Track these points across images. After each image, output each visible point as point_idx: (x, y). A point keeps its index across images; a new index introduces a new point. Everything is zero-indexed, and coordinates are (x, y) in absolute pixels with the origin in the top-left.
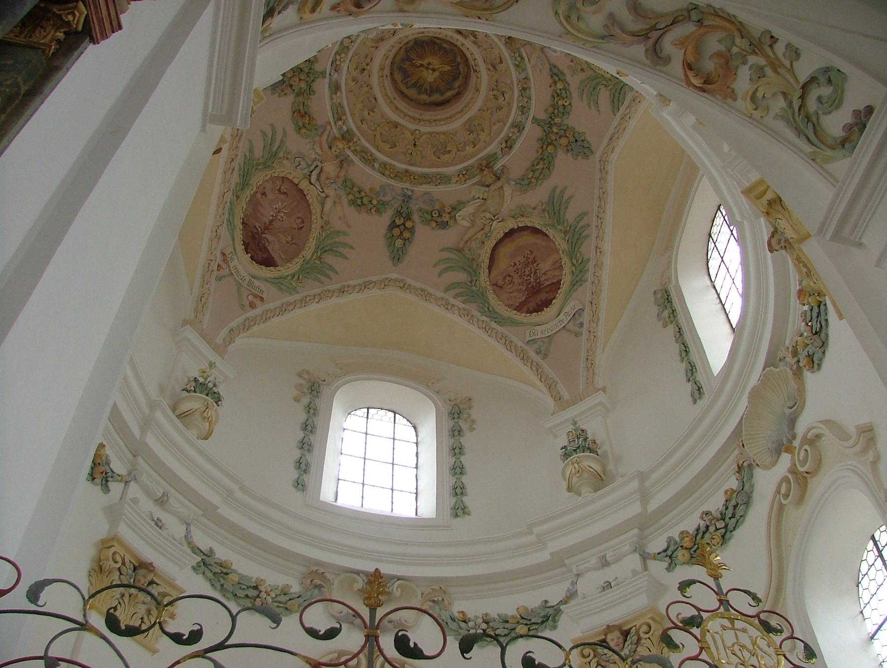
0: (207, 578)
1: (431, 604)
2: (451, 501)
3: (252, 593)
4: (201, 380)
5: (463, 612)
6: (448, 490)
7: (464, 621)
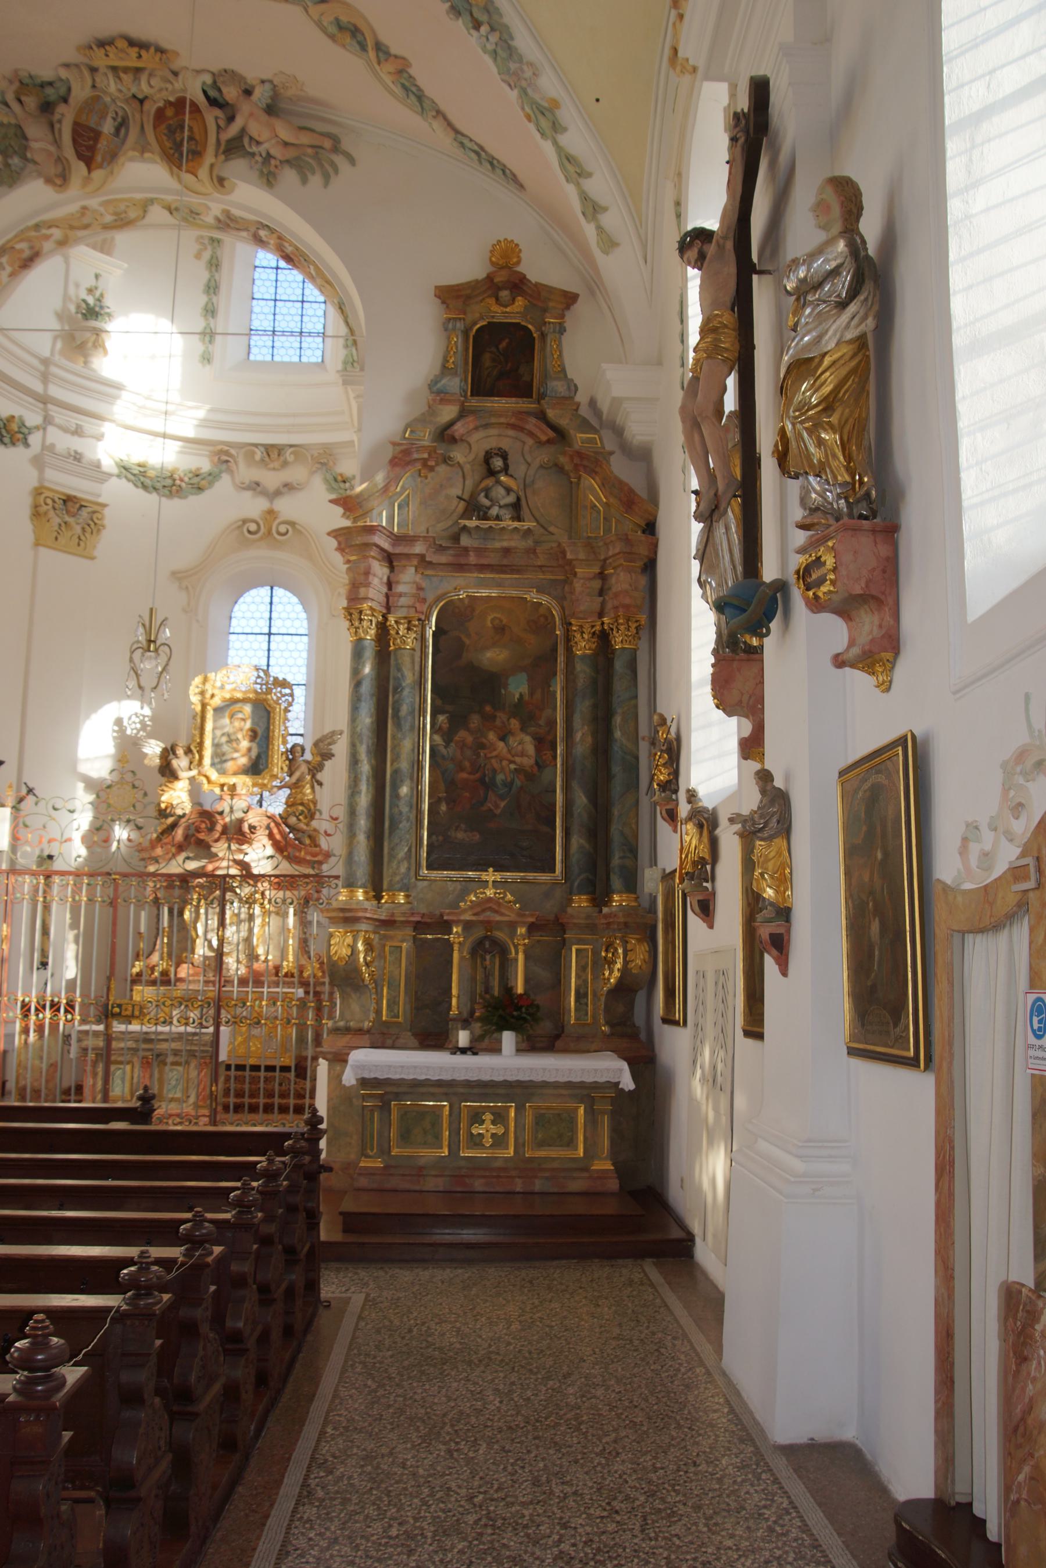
0: (129, 480)
1: (319, 466)
3: (169, 482)
4: (91, 301)
5: (341, 475)
7: (344, 482)
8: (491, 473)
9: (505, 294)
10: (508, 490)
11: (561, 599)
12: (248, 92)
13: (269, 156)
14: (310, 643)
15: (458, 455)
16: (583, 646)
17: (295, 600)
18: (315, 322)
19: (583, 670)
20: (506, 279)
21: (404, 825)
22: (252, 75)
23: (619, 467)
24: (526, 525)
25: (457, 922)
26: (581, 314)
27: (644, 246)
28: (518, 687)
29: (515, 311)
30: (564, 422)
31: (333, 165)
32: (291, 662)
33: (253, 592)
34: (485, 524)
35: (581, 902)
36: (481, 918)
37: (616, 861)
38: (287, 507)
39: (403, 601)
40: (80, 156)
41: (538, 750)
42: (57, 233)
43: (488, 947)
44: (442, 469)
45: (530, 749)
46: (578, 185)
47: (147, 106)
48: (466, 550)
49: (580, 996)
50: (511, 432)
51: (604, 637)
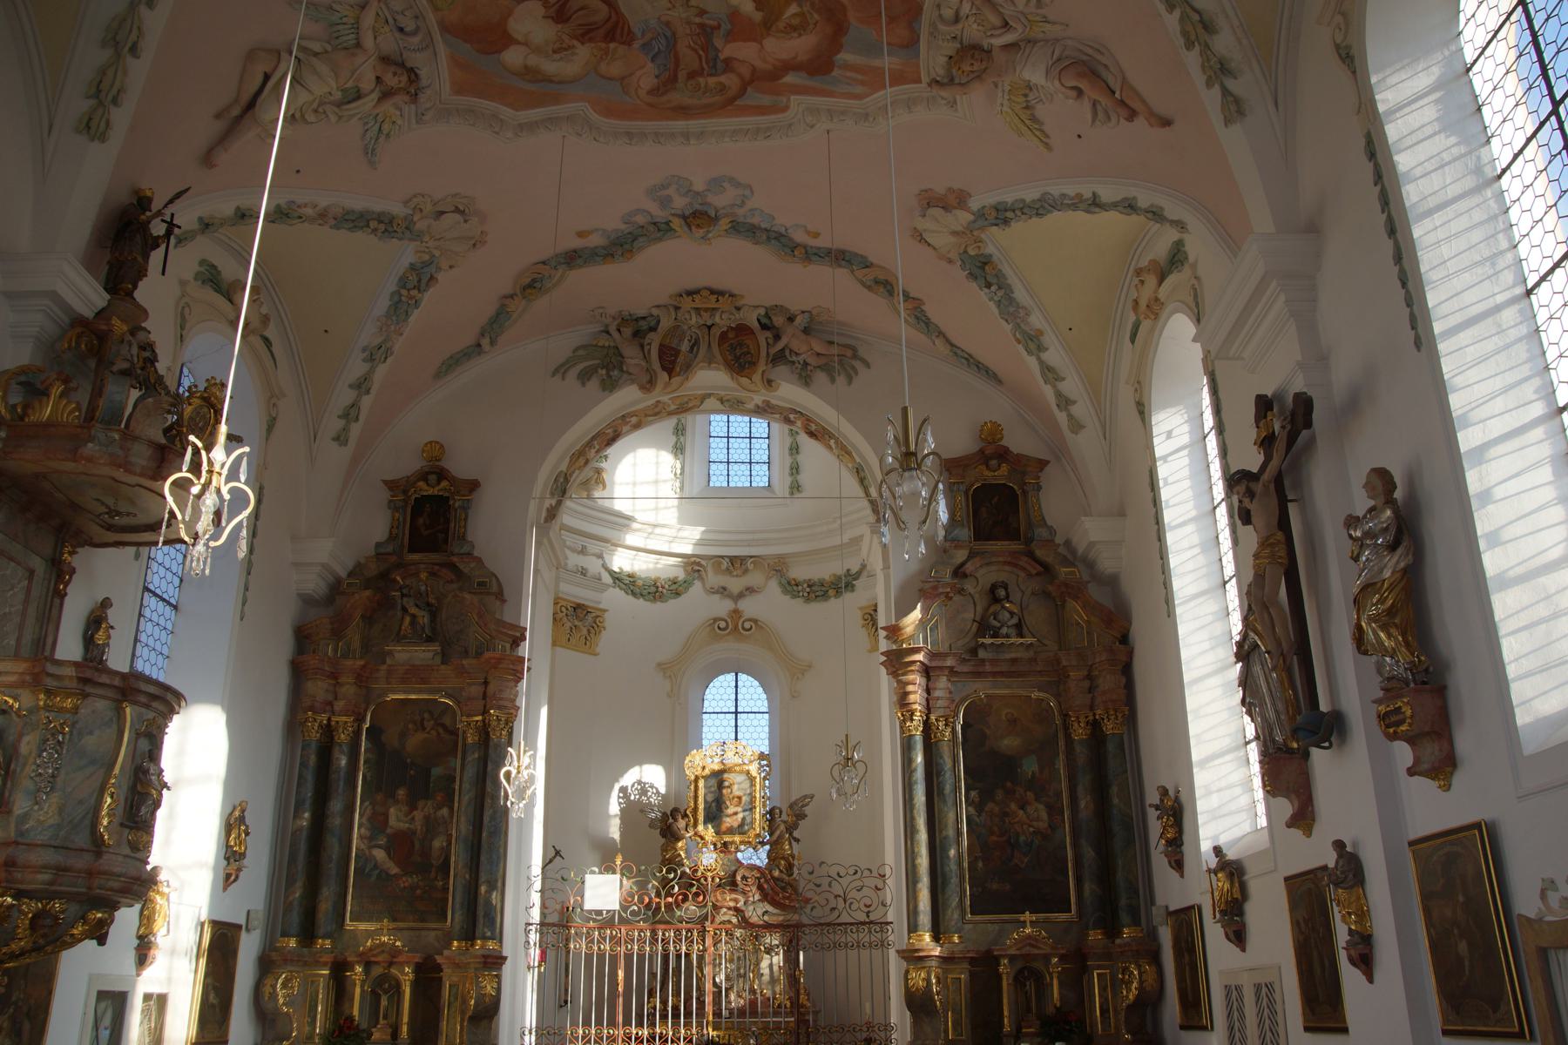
2: (789, 480)
3: (653, 589)
6: (787, 470)
8: (996, 600)
9: (994, 462)
10: (1012, 614)
11: (1057, 696)
12: (791, 319)
13: (806, 364)
14: (770, 720)
15: (969, 586)
16: (1080, 732)
17: (756, 683)
18: (761, 454)
19: (1081, 753)
20: (992, 450)
21: (954, 880)
22: (794, 308)
23: (1095, 592)
24: (1029, 640)
25: (1004, 956)
26: (1050, 477)
27: (1104, 427)
28: (1030, 766)
29: (1001, 474)
30: (1049, 559)
31: (853, 368)
32: (755, 735)
33: (721, 678)
34: (999, 641)
35: (1095, 936)
36: (1024, 951)
37: (1123, 902)
38: (749, 607)
39: (940, 703)
40: (664, 368)
41: (1049, 815)
42: (634, 420)
43: (1029, 973)
44: (957, 598)
45: (1044, 815)
46: (1054, 386)
47: (713, 331)
48: (983, 661)
49: (1104, 1011)
50: (1007, 568)
51: (1095, 725)
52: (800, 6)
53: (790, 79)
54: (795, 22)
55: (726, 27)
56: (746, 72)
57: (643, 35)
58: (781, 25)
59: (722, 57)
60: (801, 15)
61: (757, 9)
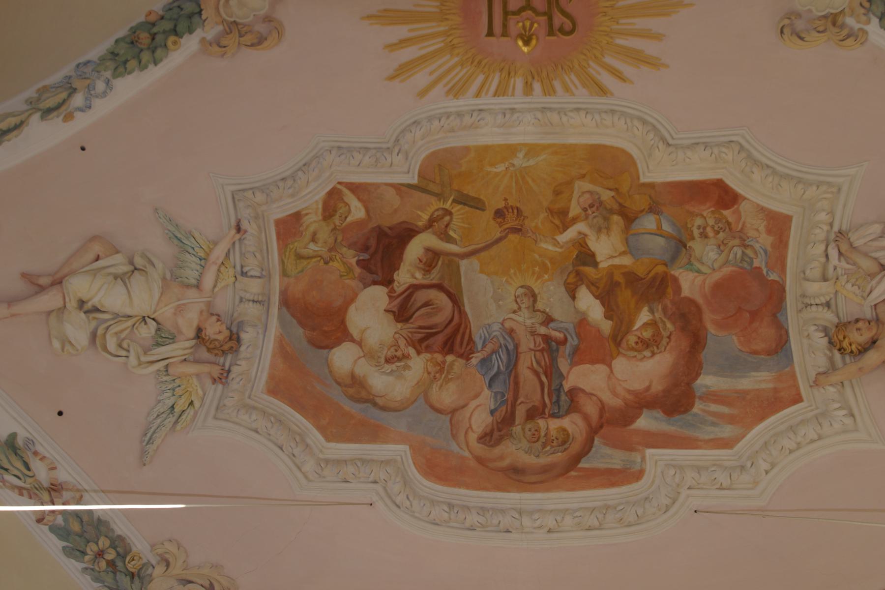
52: (651, 311)
53: (645, 422)
54: (647, 334)
55: (573, 341)
56: (591, 409)
57: (484, 346)
58: (632, 339)
59: (567, 386)
60: (653, 324)
61: (607, 317)
